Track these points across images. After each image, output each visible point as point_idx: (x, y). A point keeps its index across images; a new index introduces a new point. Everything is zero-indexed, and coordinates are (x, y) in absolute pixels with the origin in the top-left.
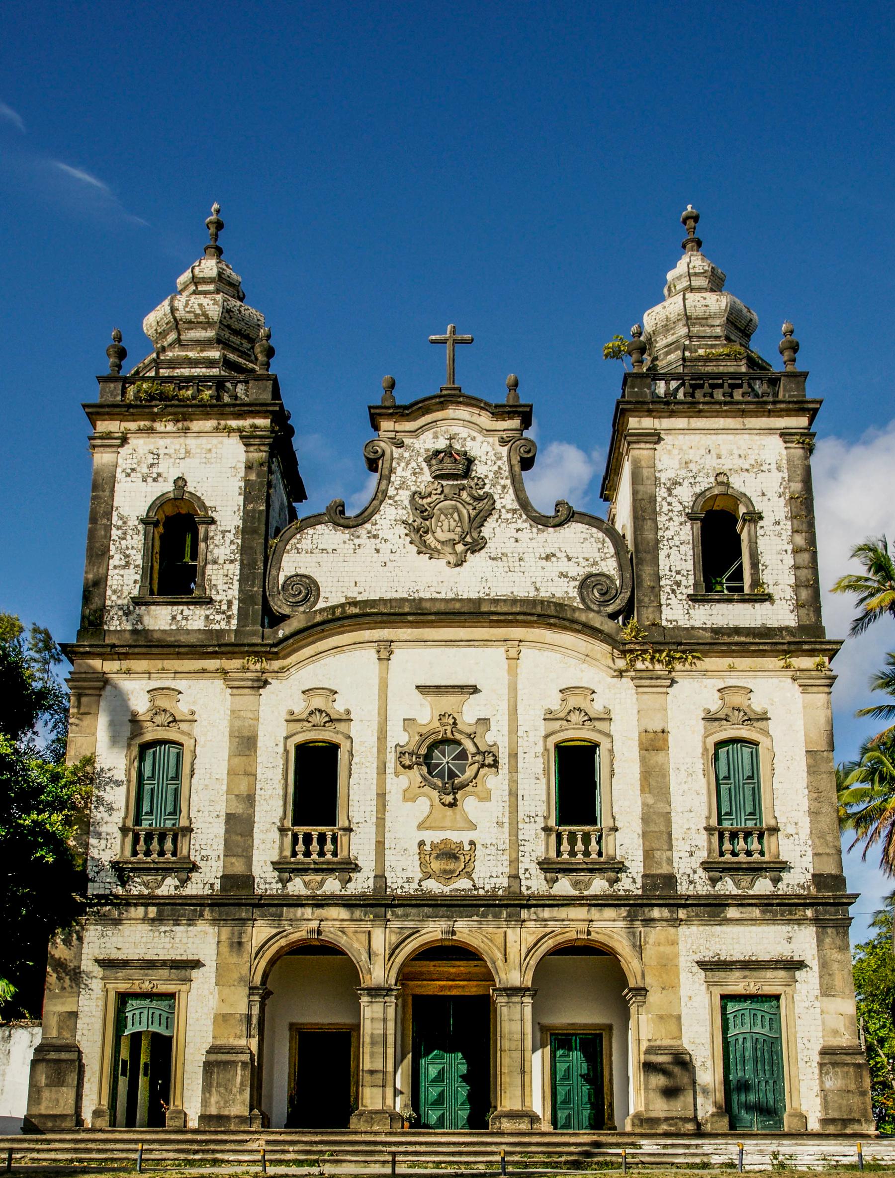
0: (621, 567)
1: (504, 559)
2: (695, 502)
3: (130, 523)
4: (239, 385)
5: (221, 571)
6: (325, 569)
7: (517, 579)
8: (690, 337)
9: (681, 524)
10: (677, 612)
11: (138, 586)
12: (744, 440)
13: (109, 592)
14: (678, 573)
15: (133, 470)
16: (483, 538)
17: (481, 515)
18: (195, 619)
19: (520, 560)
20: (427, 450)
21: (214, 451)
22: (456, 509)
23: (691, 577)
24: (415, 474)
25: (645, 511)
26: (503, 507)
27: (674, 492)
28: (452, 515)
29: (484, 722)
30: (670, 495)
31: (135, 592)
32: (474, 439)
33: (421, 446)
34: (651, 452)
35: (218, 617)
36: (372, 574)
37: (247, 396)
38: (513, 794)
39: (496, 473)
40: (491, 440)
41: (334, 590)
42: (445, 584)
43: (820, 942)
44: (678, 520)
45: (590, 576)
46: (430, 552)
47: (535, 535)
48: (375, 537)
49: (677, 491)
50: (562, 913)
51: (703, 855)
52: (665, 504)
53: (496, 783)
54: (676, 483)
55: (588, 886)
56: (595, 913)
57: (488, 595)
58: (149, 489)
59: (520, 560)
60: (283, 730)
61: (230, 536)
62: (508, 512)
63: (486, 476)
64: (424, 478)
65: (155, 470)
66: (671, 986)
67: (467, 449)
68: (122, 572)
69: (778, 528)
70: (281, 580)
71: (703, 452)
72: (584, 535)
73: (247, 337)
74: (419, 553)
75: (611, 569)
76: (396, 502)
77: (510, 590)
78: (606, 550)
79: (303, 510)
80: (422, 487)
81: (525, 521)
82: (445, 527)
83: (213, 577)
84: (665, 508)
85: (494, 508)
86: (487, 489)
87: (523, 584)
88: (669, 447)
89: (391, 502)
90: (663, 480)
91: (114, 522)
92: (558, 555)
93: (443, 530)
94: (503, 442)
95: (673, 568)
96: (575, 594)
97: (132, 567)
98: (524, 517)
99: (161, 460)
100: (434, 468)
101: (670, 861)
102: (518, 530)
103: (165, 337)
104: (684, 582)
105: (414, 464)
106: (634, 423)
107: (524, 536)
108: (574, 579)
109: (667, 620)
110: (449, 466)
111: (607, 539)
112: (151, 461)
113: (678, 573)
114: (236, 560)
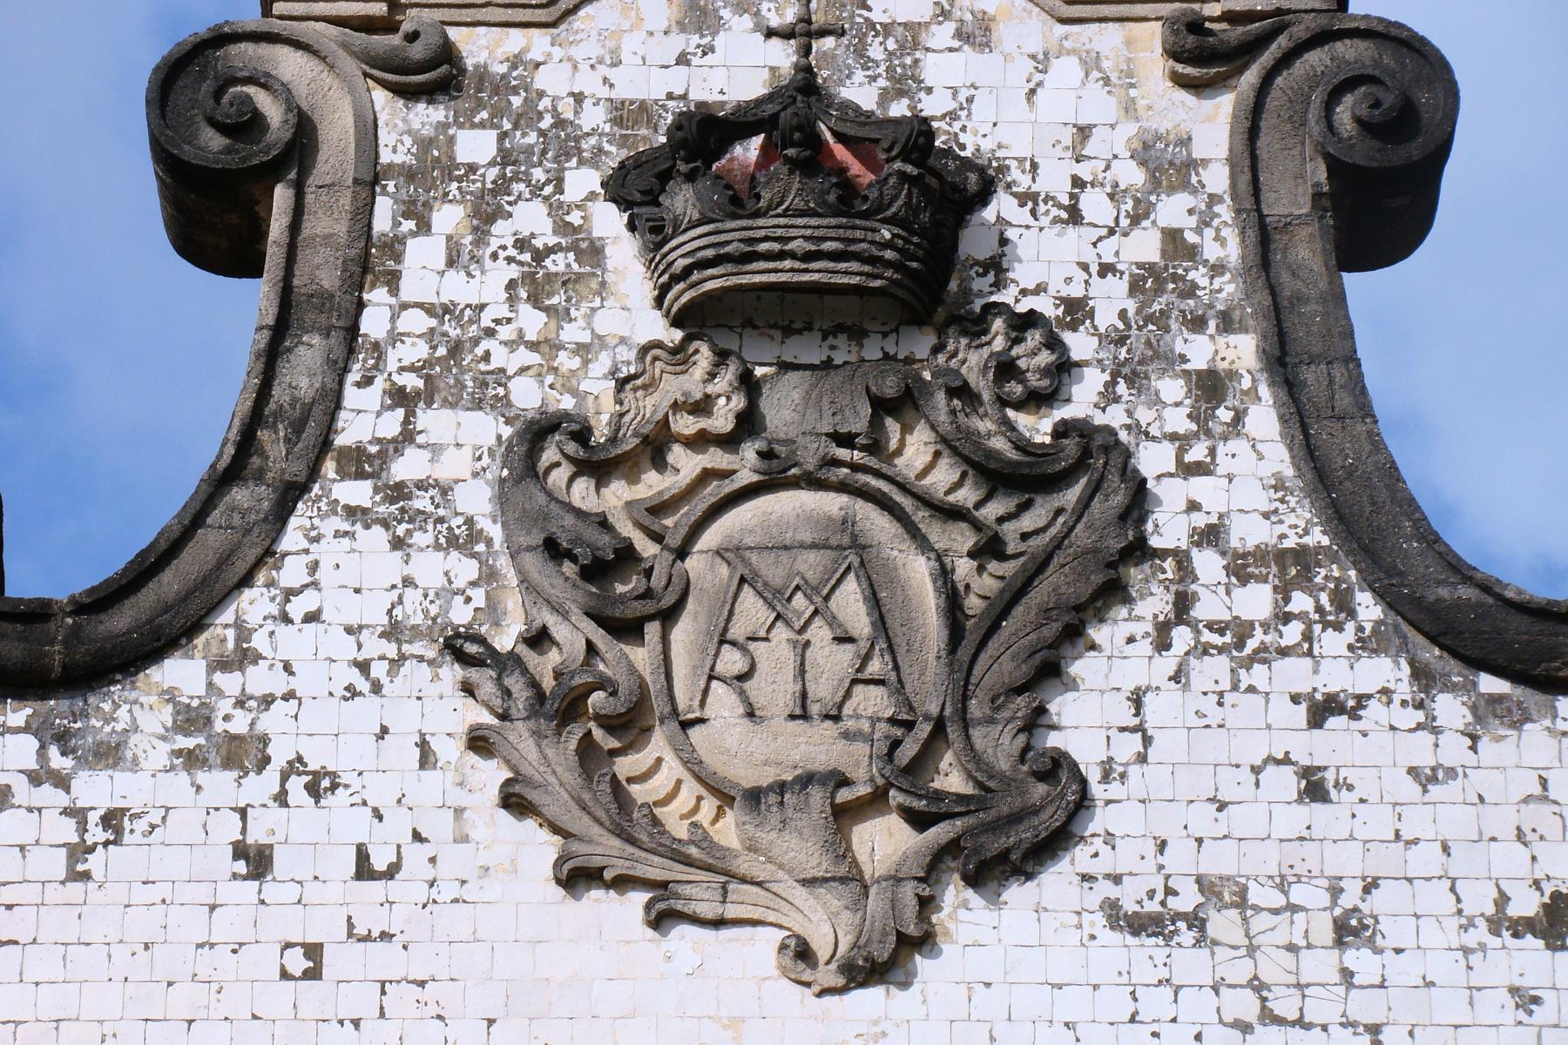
1: (1223, 924)
19: (1347, 931)
20: (627, 114)
22: (854, 552)
24: (533, 286)
26: (1211, 536)
39: (1146, 281)
40: (1107, 39)
47: (1454, 750)
48: (244, 754)
59: (1347, 931)
62: (1241, 569)
63: (1077, 311)
74: (577, 877)
81: (1366, 645)
82: (774, 686)
93: (757, 701)
98: (1369, 609)
102: (1323, 709)
105: (530, 218)
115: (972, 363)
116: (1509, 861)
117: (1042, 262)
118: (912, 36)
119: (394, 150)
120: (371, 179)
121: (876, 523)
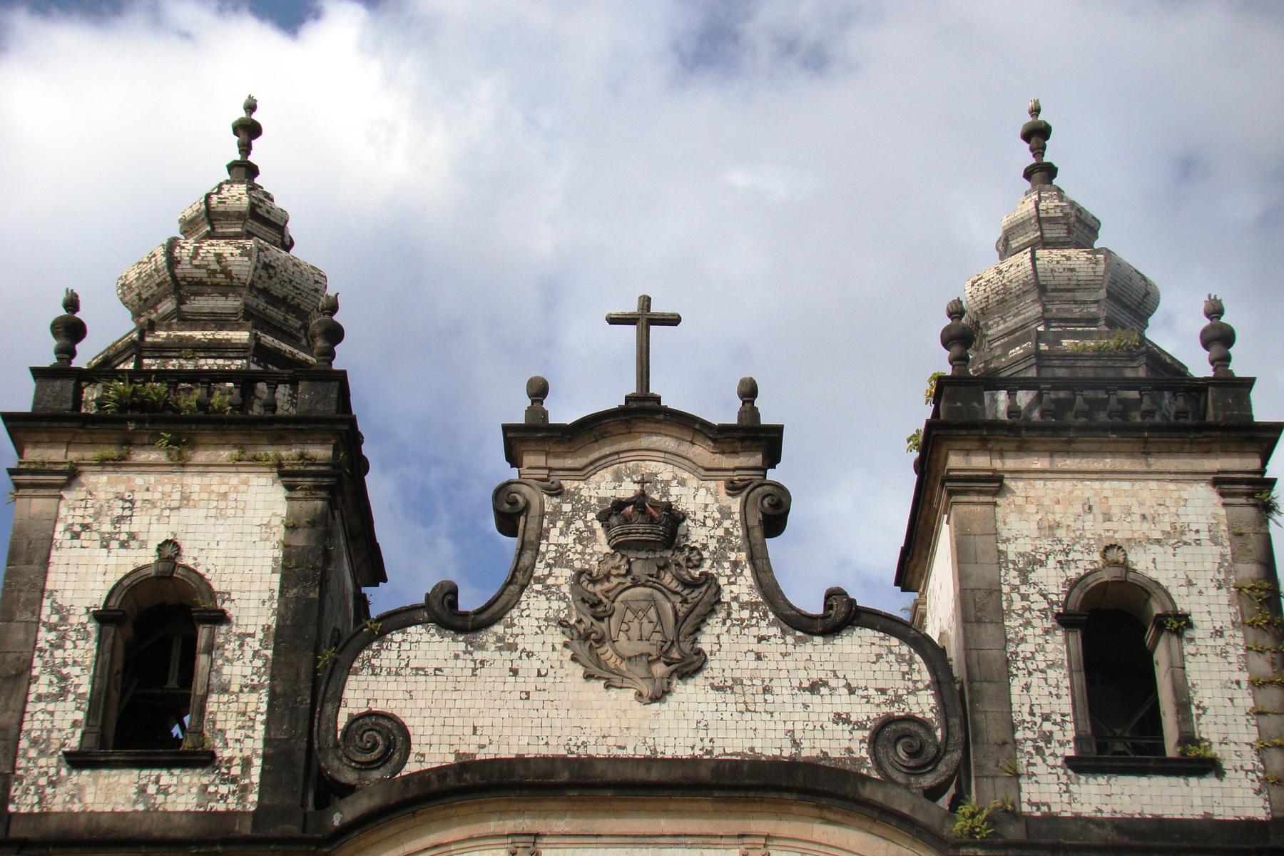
0: (943, 707)
1: (738, 689)
2: (1068, 595)
3: (74, 620)
4: (281, 388)
5: (234, 706)
6: (421, 704)
7: (760, 725)
8: (1047, 322)
9: (1047, 632)
11: (79, 732)
12: (1149, 491)
13: (24, 743)
14: (1046, 718)
15: (86, 527)
16: (700, 652)
17: (696, 612)
19: (766, 690)
20: (601, 500)
21: (232, 496)
22: (653, 601)
23: (1070, 727)
27: (1033, 577)
28: (645, 611)
30: (1025, 581)
31: (74, 743)
32: (682, 483)
33: (593, 493)
34: (988, 508)
35: (224, 789)
36: (505, 713)
37: (294, 405)
39: (721, 540)
40: (712, 485)
41: (435, 740)
42: (634, 733)
44: (1040, 624)
45: (888, 721)
46: (607, 675)
47: (790, 649)
48: (512, 647)
49: (1037, 575)
52: (1015, 596)
54: (1035, 562)
57: (709, 752)
58: (112, 561)
62: (742, 606)
63: (705, 546)
64: (597, 548)
65: (125, 528)
67: (672, 499)
68: (51, 707)
69: (1220, 642)
70: (341, 725)
71: (1078, 508)
72: (876, 649)
73: (296, 310)
74: (588, 677)
75: (927, 709)
76: (548, 587)
77: (748, 744)
78: (916, 676)
79: (381, 600)
80: (594, 562)
81: (771, 624)
82: (634, 633)
83: (220, 716)
84: (1018, 605)
85: (719, 602)
86: (706, 566)
87: (771, 734)
88: (1020, 501)
89: (538, 587)
90: (1011, 557)
91: (44, 618)
92: (833, 683)
93: (630, 636)
94: (733, 489)
95: (1036, 710)
96: (864, 754)
97: (71, 697)
98: (771, 616)
99: (137, 512)
100: (614, 531)
102: (761, 639)
103: (154, 307)
104: (1058, 735)
105: (579, 524)
107: (772, 649)
108: (861, 726)
109: (1030, 803)
110: (641, 528)
111: (917, 657)
112: (118, 512)
113: (1046, 718)
114: (262, 686)
115: (681, 558)
116: (802, 674)
117: (697, 535)
118: (667, 483)
119: (548, 508)
120: (543, 515)
121: (659, 595)
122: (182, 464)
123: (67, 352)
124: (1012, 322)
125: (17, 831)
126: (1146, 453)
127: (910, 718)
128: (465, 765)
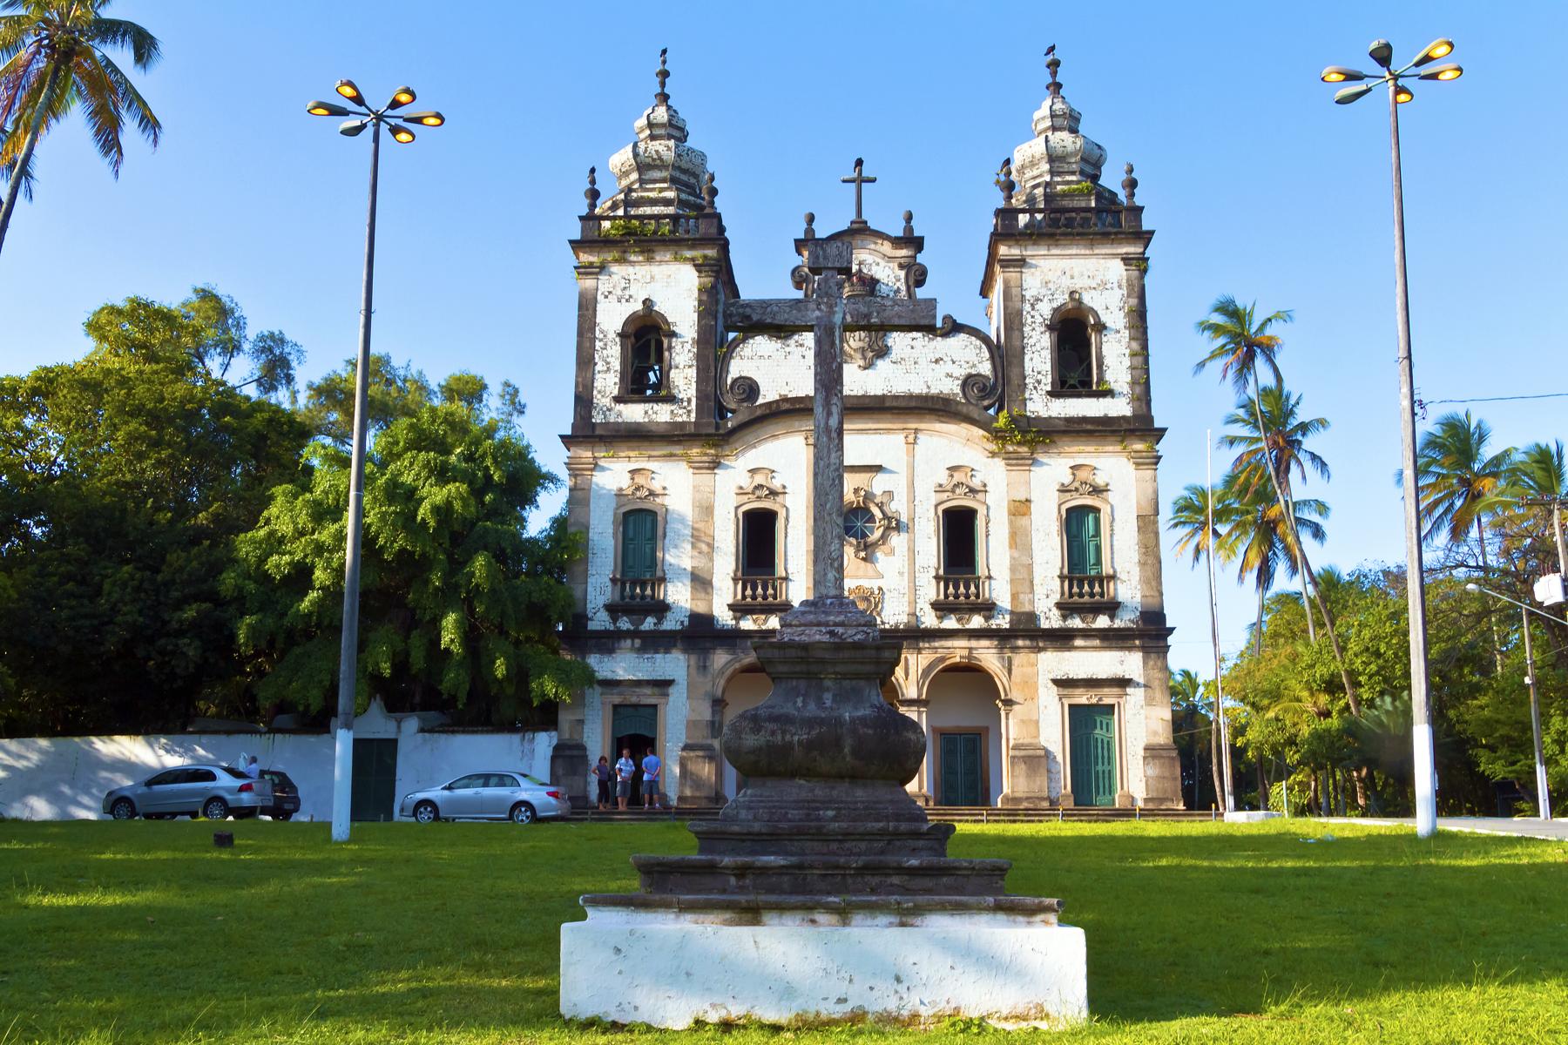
10: (1041, 405)
18: (662, 414)
25: (1013, 321)
29: (890, 494)
31: (616, 392)
38: (912, 552)
43: (1145, 663)
45: (970, 376)
49: (1039, 306)
50: (949, 643)
51: (1056, 597)
53: (897, 540)
54: (1038, 300)
55: (969, 621)
56: (974, 643)
60: (734, 501)
61: (688, 346)
65: (627, 292)
66: (1033, 697)
84: (1029, 320)
94: (901, 266)
101: (1032, 602)
106: (1003, 250)
122: (650, 260)
123: (593, 206)
124: (1036, 172)
125: (598, 432)
126: (1092, 246)
127: (979, 375)
128: (785, 399)
